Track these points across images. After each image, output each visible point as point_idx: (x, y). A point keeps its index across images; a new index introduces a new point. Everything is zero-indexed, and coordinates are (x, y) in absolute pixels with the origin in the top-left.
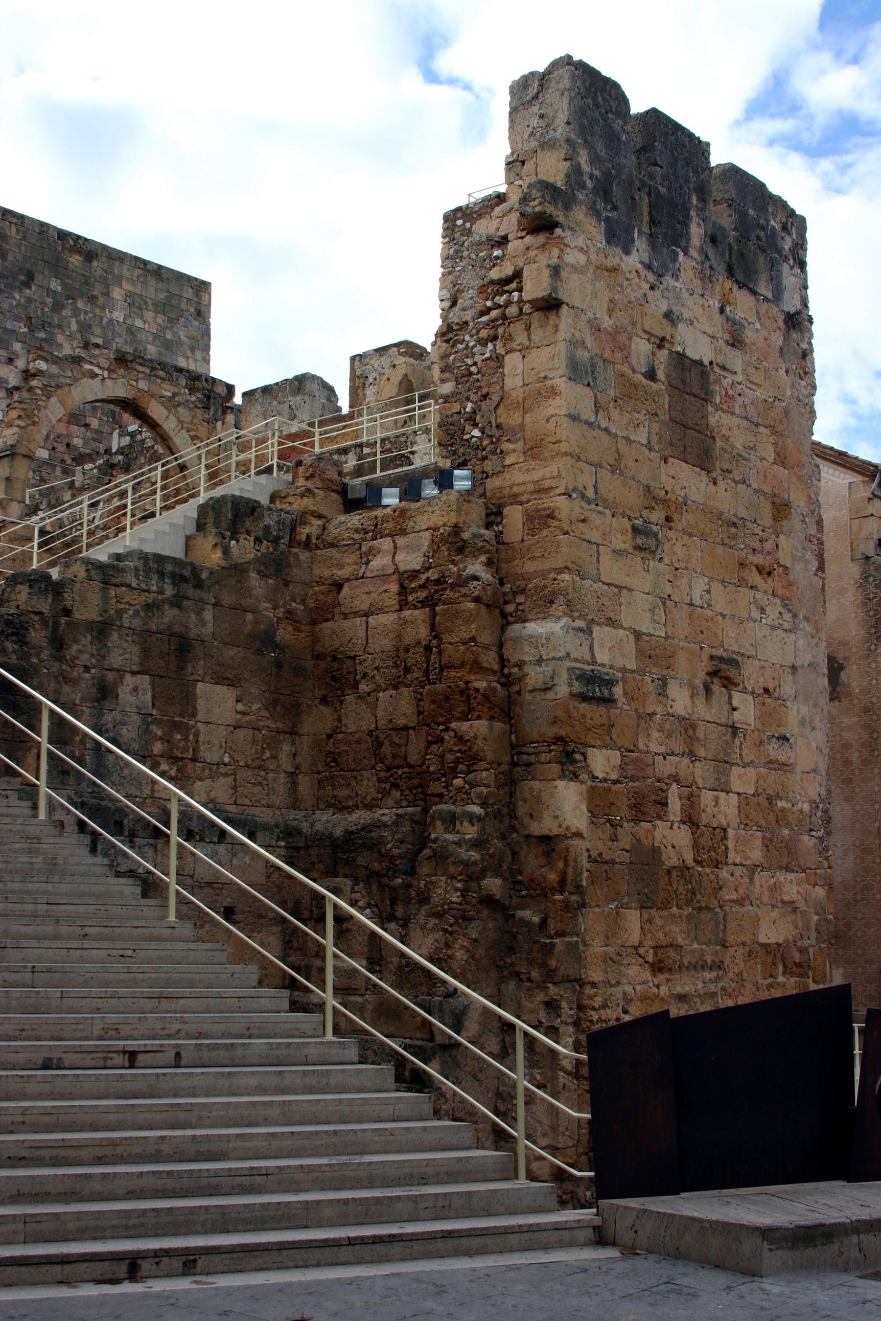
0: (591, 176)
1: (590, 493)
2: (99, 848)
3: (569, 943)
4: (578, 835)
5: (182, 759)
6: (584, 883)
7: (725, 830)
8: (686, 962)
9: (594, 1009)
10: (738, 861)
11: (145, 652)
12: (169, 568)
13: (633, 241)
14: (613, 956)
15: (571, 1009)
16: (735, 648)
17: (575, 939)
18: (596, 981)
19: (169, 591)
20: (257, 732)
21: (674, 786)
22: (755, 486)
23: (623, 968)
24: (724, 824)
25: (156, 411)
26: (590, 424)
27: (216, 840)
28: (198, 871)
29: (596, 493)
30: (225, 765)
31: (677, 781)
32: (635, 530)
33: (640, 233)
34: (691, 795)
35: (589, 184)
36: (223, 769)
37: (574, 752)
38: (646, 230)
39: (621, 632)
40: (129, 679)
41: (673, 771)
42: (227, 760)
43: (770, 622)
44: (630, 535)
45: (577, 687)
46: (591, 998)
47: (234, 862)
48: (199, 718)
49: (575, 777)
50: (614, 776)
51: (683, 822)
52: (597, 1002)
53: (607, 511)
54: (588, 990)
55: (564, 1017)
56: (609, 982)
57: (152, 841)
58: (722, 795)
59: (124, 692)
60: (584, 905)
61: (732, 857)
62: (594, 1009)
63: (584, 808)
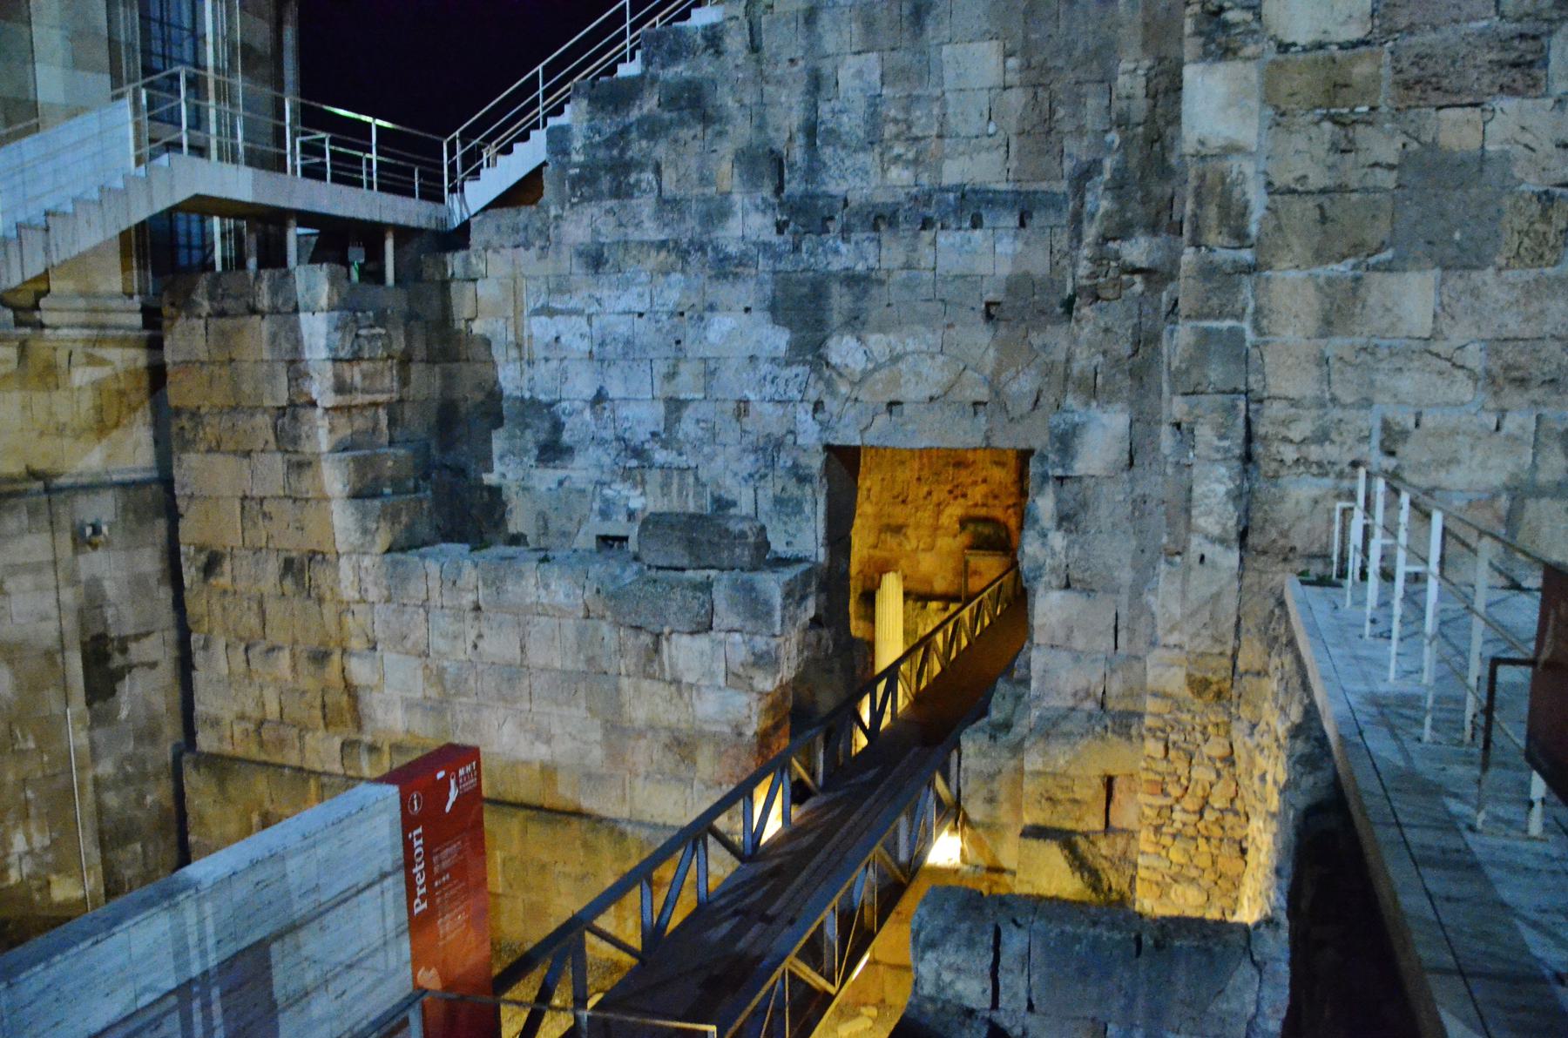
2: (804, 248)
3: (1207, 334)
4: (1231, 149)
5: (924, 138)
6: (1253, 229)
9: (1286, 440)
11: (869, 25)
14: (1348, 355)
15: (1222, 437)
17: (1228, 323)
18: (1292, 393)
20: (1040, 90)
23: (1379, 378)
27: (967, 224)
28: (940, 261)
30: (990, 136)
36: (986, 141)
37: (1221, 9)
40: (853, 62)
42: (992, 129)
46: (1285, 423)
47: (998, 249)
48: (946, 87)
49: (1228, 53)
50: (1355, 32)
52: (1296, 433)
54: (1275, 410)
55: (1201, 449)
56: (1334, 399)
57: (872, 235)
59: (845, 76)
62: (1286, 440)
63: (1254, 103)
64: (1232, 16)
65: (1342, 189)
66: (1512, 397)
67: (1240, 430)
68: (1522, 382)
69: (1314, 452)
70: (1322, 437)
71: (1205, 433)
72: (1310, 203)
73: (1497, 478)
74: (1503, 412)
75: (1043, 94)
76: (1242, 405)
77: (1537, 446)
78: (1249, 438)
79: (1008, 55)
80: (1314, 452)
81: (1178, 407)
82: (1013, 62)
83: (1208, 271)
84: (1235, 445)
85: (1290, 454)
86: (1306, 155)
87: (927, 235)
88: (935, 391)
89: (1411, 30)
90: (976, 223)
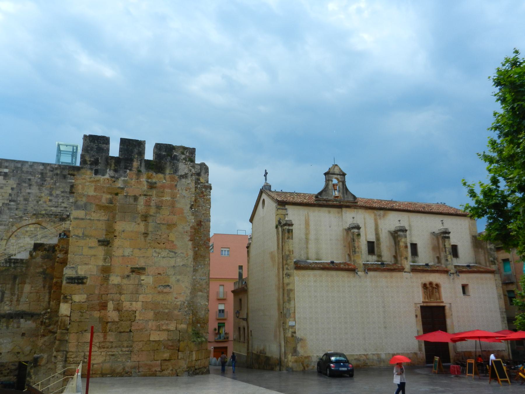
0: (90, 161)
1: (81, 235)
7: (136, 311)
8: (114, 346)
10: (141, 319)
12: (13, 261)
13: (106, 172)
16: (144, 264)
19: (12, 265)
21: (111, 302)
22: (158, 222)
24: (134, 309)
25: (44, 224)
26: (82, 219)
29: (83, 234)
31: (113, 300)
32: (99, 241)
33: (110, 170)
34: (118, 304)
35: (89, 163)
38: (112, 168)
39: (90, 266)
41: (111, 297)
43: (162, 256)
44: (97, 242)
45: (68, 281)
49: (66, 302)
50: (84, 301)
51: (114, 310)
52: (73, 356)
53: (87, 238)
58: (134, 303)
60: (67, 333)
61: (137, 318)
64: (68, 297)
65: (81, 322)
66: (102, 350)
67: (65, 356)
68: (104, 348)
69: (75, 359)
70: (76, 357)
71: (59, 357)
72: (77, 323)
73: (100, 361)
74: (101, 352)
75: (38, 294)
76: (65, 352)
77: (106, 357)
78: (66, 358)
79: (32, 287)
80: (75, 359)
81: (55, 353)
82: (32, 289)
83: (62, 333)
84: (63, 359)
85: (72, 360)
86: (76, 317)
87: (11, 320)
88: (9, 350)
89: (91, 301)
90: (22, 318)
